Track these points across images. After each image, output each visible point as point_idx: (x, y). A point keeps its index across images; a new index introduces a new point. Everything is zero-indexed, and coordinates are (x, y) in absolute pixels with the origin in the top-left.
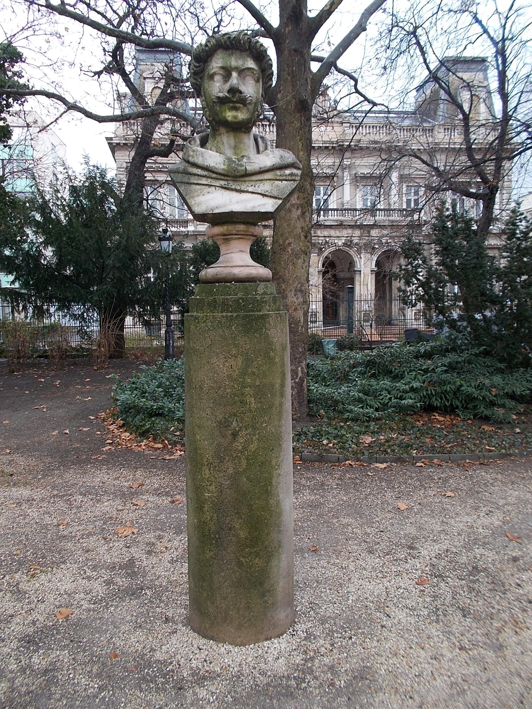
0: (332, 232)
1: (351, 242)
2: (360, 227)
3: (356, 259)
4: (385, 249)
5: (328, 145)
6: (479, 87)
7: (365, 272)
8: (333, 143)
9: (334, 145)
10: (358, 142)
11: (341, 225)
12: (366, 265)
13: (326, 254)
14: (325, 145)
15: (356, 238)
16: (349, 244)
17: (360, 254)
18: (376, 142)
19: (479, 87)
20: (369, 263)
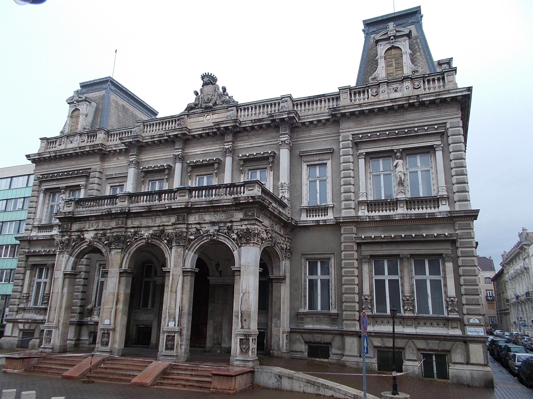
0: (145, 222)
1: (163, 231)
2: (169, 211)
3: (167, 256)
4: (205, 240)
5: (207, 131)
6: (395, 37)
7: (175, 273)
8: (213, 129)
9: (214, 130)
10: (235, 122)
11: (150, 212)
12: (178, 262)
13: (133, 249)
14: (205, 132)
15: (169, 227)
16: (160, 234)
17: (171, 248)
18: (259, 120)
19: (395, 37)
20: (180, 260)
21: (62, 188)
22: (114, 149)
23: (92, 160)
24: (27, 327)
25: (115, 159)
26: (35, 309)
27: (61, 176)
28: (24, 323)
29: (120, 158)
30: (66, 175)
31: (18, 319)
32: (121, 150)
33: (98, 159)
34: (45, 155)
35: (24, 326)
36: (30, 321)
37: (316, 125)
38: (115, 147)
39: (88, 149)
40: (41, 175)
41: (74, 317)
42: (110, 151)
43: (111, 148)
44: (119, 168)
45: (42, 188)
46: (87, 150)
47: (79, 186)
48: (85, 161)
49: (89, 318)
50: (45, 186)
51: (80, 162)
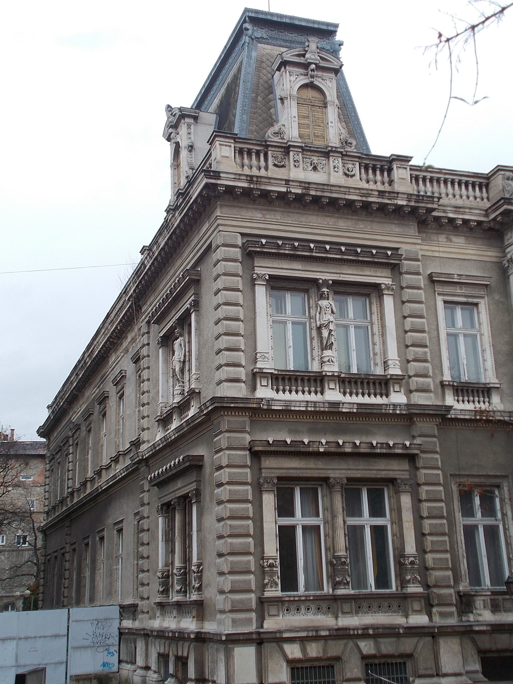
21: (325, 281)
22: (451, 215)
23: (396, 229)
24: (314, 650)
25: (442, 238)
26: (318, 599)
27: (326, 251)
28: (302, 641)
29: (454, 239)
30: (342, 253)
31: (280, 632)
32: (466, 222)
33: (412, 229)
34: (270, 184)
35: (304, 650)
36: (323, 633)
37: (471, 229)
38: (455, 212)
39: (404, 203)
40: (242, 235)
41: (451, 614)
42: (437, 219)
43: (444, 211)
44: (458, 262)
45: (258, 271)
46: (400, 202)
47: (376, 287)
48: (376, 227)
49: (471, 618)
50: (265, 268)
51: (361, 226)
